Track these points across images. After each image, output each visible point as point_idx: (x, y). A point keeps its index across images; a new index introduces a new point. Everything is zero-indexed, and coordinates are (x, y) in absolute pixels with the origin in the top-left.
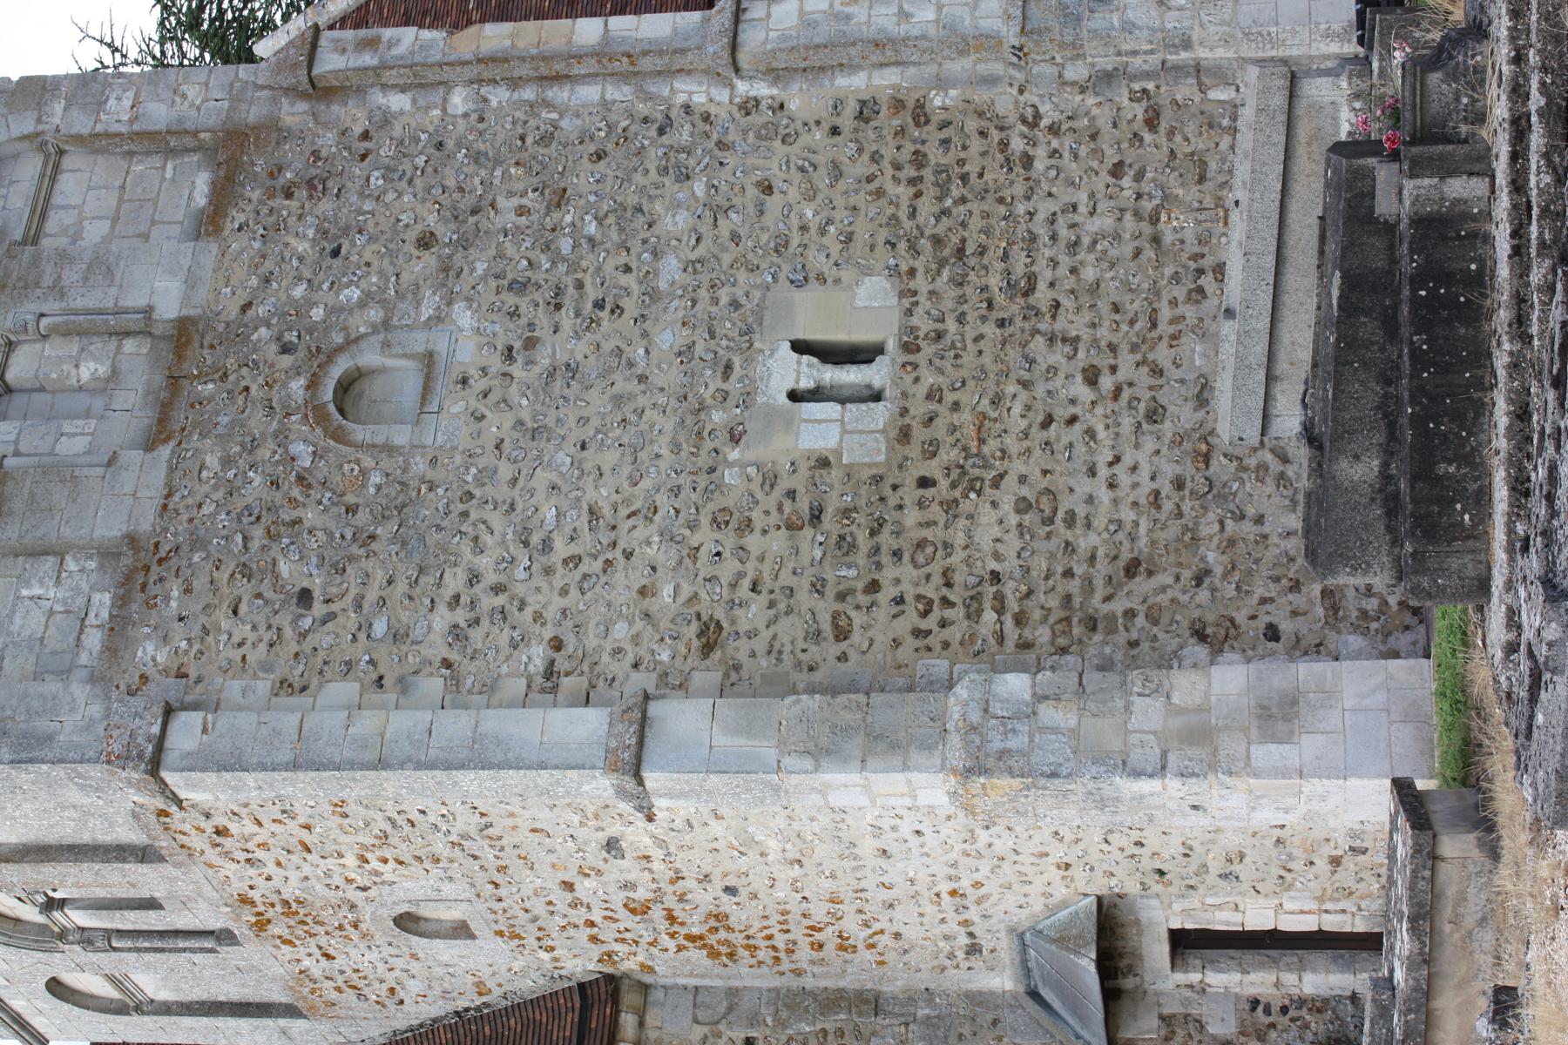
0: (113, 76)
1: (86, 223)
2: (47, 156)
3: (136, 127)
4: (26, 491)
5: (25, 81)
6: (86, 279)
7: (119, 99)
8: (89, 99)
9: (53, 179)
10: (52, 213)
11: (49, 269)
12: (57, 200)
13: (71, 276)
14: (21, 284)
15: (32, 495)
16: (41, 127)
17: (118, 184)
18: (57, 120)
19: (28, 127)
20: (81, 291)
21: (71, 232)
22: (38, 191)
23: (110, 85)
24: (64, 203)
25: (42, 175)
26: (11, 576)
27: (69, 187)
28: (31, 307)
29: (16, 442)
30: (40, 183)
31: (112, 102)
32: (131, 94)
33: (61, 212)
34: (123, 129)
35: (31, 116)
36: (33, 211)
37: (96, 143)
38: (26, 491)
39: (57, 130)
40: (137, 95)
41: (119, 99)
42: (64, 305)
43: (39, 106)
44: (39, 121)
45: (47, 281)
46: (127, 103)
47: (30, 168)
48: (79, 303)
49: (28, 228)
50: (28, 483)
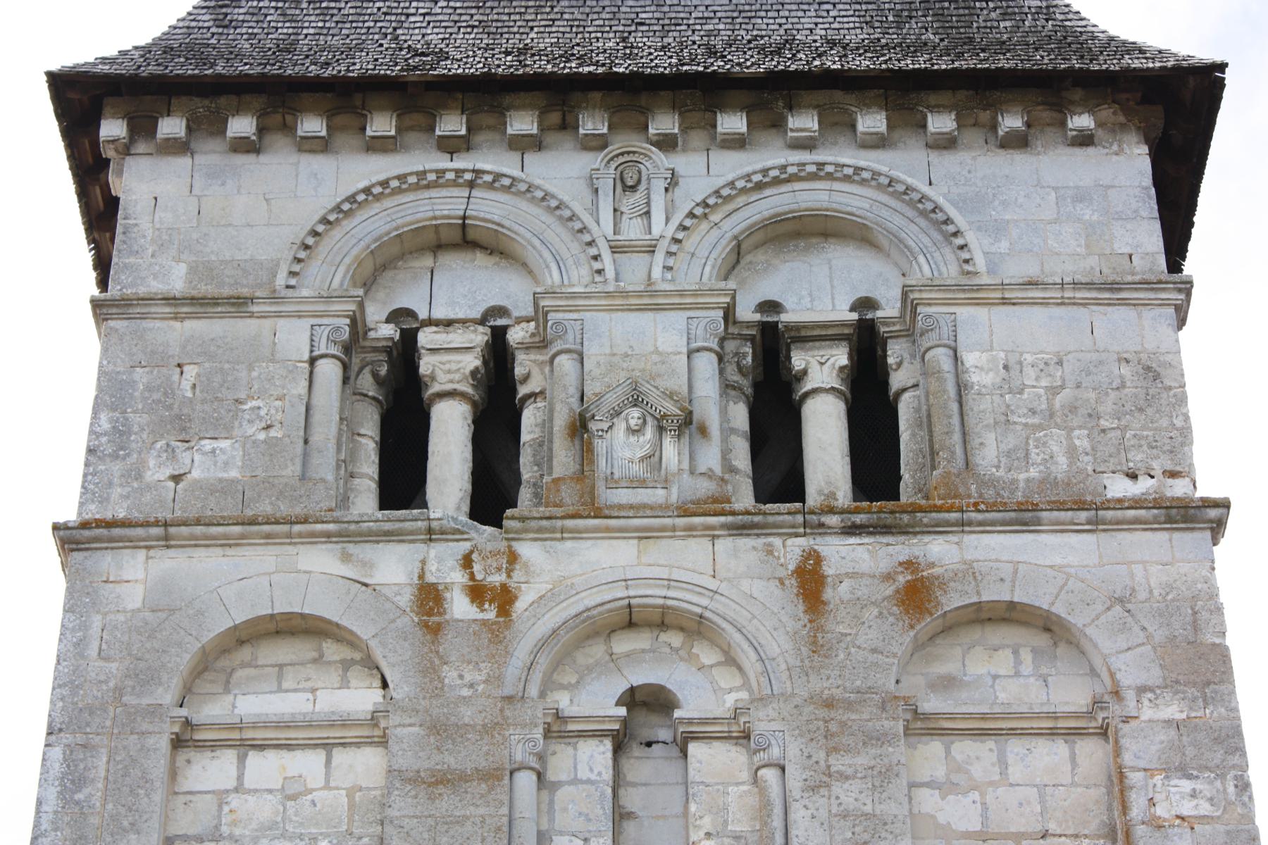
0: (272, 828)
1: (975, 795)
2: (1090, 715)
3: (1140, 830)
4: (471, 810)
5: (1223, 655)
6: (845, 816)
7: (1194, 794)
8: (1190, 752)
9: (1052, 733)
10: (990, 743)
11: (862, 760)
12: (1015, 747)
13: (849, 795)
14: (833, 727)
15: (462, 821)
16: (1130, 696)
17: (1053, 827)
18: (1147, 713)
19: (1128, 679)
20: (823, 814)
21: (955, 778)
22: (1021, 716)
23: (1222, 777)
24: (1011, 758)
25: (1054, 716)
26: (351, 820)
27: (1048, 757)
28: (794, 751)
29: (575, 781)
30: (1038, 716)
31: (1187, 785)
32: (1205, 808)
33: (994, 757)
34: (1136, 812)
35: (1154, 676)
36: (983, 717)
37: (1118, 783)
38: (471, 810)
39: (1126, 720)
40: (1203, 819)
41: (1194, 794)
42: (796, 794)
43: (1173, 685)
44: (1142, 690)
45: (839, 763)
46: (1187, 808)
47: (1070, 694)
48: (799, 814)
49: (951, 717)
50: (482, 811)
